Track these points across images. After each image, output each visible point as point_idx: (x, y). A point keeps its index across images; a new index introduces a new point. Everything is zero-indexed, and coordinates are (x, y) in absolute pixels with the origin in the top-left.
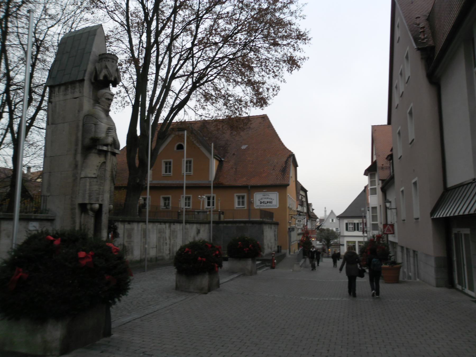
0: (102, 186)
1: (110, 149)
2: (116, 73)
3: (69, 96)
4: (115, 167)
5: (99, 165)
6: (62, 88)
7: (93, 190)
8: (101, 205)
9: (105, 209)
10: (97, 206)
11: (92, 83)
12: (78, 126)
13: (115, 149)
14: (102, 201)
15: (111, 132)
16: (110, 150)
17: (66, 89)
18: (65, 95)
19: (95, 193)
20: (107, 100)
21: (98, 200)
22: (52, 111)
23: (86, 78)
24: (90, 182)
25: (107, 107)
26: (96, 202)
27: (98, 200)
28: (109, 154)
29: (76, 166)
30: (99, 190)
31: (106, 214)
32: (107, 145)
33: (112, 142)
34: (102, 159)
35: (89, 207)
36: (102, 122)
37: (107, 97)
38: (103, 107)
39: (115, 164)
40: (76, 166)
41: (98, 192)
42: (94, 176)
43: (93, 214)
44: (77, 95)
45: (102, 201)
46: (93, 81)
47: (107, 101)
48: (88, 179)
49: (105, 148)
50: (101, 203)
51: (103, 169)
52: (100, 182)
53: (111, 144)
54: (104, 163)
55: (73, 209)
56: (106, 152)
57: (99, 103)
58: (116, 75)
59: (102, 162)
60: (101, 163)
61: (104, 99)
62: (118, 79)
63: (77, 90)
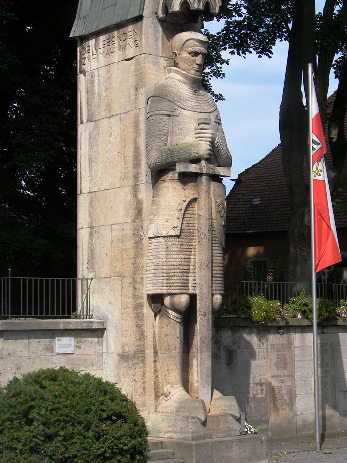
0: (193, 253)
3: (117, 56)
5: (184, 207)
6: (103, 38)
8: (193, 297)
9: (202, 306)
10: (184, 300)
11: (162, 21)
12: (136, 124)
13: (219, 166)
14: (194, 287)
17: (110, 41)
18: (109, 53)
19: (178, 271)
20: (193, 56)
21: (188, 286)
22: (88, 92)
23: (146, 12)
24: (168, 247)
25: (193, 72)
27: (185, 285)
28: (204, 179)
29: (139, 212)
32: (197, 160)
33: (208, 152)
34: (189, 192)
35: (167, 301)
37: (190, 49)
38: (185, 73)
40: (139, 212)
41: (185, 267)
42: (173, 233)
44: (130, 52)
45: (194, 287)
46: (161, 15)
47: (193, 58)
48: (161, 239)
49: (193, 168)
52: (188, 245)
53: (205, 157)
55: (138, 307)
57: (176, 65)
59: (188, 200)
60: (187, 203)
61: (185, 55)
63: (130, 41)
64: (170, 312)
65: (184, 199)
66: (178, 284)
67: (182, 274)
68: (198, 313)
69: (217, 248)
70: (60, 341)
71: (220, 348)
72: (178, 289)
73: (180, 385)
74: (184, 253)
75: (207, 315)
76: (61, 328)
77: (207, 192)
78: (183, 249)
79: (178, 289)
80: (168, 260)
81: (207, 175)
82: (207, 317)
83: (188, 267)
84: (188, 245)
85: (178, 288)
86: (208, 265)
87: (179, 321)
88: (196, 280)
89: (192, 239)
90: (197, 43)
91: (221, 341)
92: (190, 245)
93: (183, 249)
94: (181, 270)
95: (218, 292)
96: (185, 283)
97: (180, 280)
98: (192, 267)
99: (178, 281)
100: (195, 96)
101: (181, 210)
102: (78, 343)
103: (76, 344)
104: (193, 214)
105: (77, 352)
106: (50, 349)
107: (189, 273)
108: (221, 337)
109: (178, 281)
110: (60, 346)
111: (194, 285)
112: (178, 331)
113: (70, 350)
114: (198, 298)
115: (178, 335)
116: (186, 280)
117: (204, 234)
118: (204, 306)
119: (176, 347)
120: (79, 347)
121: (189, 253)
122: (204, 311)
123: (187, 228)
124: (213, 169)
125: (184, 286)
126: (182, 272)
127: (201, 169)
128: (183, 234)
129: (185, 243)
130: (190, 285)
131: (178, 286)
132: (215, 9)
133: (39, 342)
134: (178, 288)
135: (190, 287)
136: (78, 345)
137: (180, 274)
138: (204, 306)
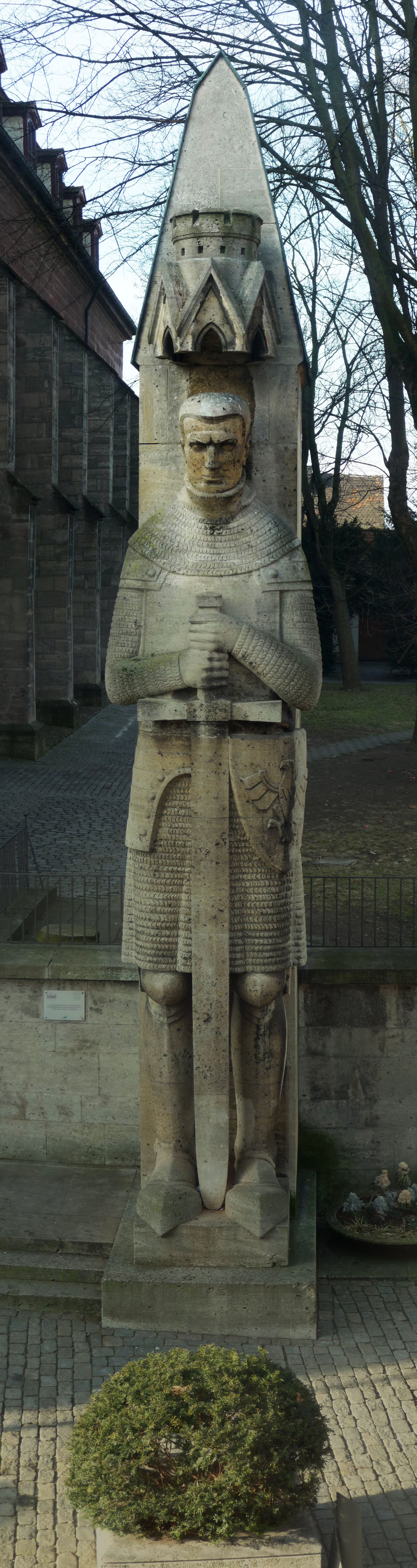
0: (184, 888)
8: (187, 978)
14: (185, 958)
20: (197, 450)
27: (166, 954)
31: (207, 1021)
45: (185, 958)
51: (182, 812)
52: (172, 871)
59: (168, 779)
62: (225, 329)
69: (254, 876)
70: (54, 997)
73: (172, 1145)
75: (213, 1021)
76: (46, 977)
77: (211, 761)
81: (208, 723)
82: (213, 1023)
84: (172, 871)
86: (215, 917)
88: (190, 945)
89: (183, 859)
90: (199, 424)
95: (258, 968)
98: (182, 917)
99: (148, 945)
100: (210, 538)
101: (153, 798)
102: (95, 1003)
103: (90, 1004)
104: (182, 808)
105: (94, 1018)
110: (54, 1007)
112: (165, 1041)
114: (194, 982)
115: (165, 1048)
116: (169, 943)
117: (204, 851)
118: (205, 1002)
119: (161, 1072)
120: (98, 1011)
122: (205, 1010)
125: (163, 956)
126: (158, 928)
127: (192, 712)
128: (160, 849)
129: (165, 869)
130: (180, 955)
132: (233, 343)
133: (8, 997)
136: (96, 1007)
137: (152, 932)
138: (205, 1002)
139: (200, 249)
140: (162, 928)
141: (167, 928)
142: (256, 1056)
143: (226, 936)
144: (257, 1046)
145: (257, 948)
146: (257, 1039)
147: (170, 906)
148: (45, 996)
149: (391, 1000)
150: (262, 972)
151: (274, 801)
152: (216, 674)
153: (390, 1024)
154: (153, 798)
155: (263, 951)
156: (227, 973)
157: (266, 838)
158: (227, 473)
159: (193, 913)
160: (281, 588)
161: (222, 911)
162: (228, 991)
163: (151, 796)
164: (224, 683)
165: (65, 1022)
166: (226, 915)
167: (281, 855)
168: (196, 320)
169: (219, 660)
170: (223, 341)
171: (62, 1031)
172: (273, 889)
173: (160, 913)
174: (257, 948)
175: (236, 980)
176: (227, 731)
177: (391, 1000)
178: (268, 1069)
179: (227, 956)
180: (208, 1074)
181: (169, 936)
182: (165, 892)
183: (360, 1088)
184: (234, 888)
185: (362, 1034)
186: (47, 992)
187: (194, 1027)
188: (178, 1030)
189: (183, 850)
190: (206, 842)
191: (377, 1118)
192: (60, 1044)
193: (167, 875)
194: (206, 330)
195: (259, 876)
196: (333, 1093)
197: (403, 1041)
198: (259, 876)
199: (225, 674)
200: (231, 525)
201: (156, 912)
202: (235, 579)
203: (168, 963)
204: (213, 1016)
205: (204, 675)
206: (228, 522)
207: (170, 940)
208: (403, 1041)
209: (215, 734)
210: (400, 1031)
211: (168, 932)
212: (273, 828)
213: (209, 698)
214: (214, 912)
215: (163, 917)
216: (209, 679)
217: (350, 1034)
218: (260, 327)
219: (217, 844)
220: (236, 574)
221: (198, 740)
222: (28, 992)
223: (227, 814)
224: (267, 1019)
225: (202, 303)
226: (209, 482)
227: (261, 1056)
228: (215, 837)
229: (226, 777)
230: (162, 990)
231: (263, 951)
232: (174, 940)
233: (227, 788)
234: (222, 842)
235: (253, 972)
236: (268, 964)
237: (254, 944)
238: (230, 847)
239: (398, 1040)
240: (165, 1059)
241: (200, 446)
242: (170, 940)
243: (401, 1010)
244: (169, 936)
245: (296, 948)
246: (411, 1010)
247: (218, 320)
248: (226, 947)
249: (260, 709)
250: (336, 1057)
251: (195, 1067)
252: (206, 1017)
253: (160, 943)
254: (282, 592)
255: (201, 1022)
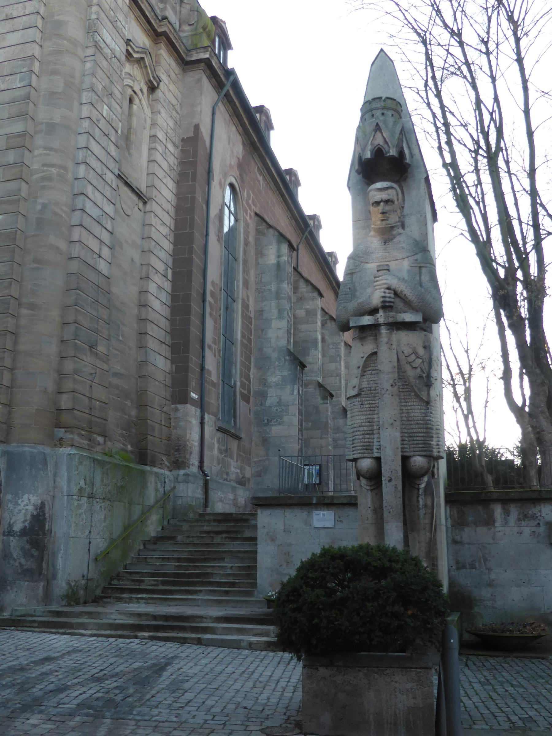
0: (376, 412)
1: (381, 317)
2: (379, 135)
4: (413, 357)
7: (355, 425)
8: (378, 460)
14: (378, 449)
15: (379, 277)
16: (381, 321)
19: (359, 433)
20: (375, 207)
21: (372, 450)
25: (379, 222)
26: (364, 453)
27: (368, 448)
30: (367, 424)
34: (369, 347)
36: (367, 263)
37: (372, 201)
39: (407, 351)
43: (367, 485)
45: (378, 449)
49: (367, 320)
50: (376, 455)
51: (374, 372)
52: (369, 404)
53: (380, 305)
54: (376, 353)
56: (375, 327)
58: (379, 140)
59: (366, 356)
60: (364, 359)
61: (372, 208)
62: (386, 146)
64: (361, 478)
65: (362, 356)
66: (359, 448)
67: (362, 436)
68: (383, 479)
69: (412, 404)
70: (318, 514)
71: (539, 524)
72: (359, 453)
74: (365, 413)
75: (393, 481)
76: (314, 502)
77: (387, 343)
78: (363, 410)
79: (359, 453)
80: (353, 422)
81: (385, 324)
82: (393, 483)
83: (371, 428)
84: (369, 404)
85: (359, 451)
86: (392, 424)
87: (368, 488)
91: (540, 516)
92: (372, 404)
93: (363, 410)
94: (361, 433)
96: (367, 446)
97: (361, 442)
98: (375, 428)
99: (359, 444)
100: (384, 246)
102: (340, 518)
103: (337, 518)
104: (373, 370)
106: (308, 523)
107: (373, 434)
108: (540, 511)
109: (359, 444)
111: (378, 447)
113: (330, 524)
114: (382, 461)
116: (369, 442)
117: (385, 390)
119: (368, 518)
120: (341, 521)
121: (371, 412)
123: (367, 386)
124: (393, 317)
125: (367, 449)
126: (363, 435)
128: (363, 393)
129: (366, 403)
130: (375, 447)
131: (359, 450)
132: (389, 152)
134: (359, 451)
135: (375, 450)
136: (340, 520)
137: (361, 437)
139: (373, 115)
140: (365, 434)
141: (368, 434)
142: (418, 506)
143: (398, 434)
144: (418, 501)
145: (415, 442)
146: (418, 497)
147: (369, 422)
148: (314, 514)
149: (498, 510)
150: (419, 456)
151: (421, 363)
152: (387, 299)
153: (497, 524)
154: (359, 367)
155: (419, 444)
156: (400, 454)
157: (417, 382)
158: (390, 216)
159: (381, 423)
160: (419, 265)
161: (395, 421)
162: (400, 464)
163: (358, 366)
164: (392, 304)
165: (325, 528)
166: (398, 423)
167: (426, 393)
168: (372, 144)
169: (389, 293)
170: (384, 151)
171: (323, 532)
172: (423, 411)
173: (364, 426)
174: (415, 442)
175: (405, 459)
176: (395, 328)
177: (498, 510)
178: (425, 514)
179: (400, 446)
180: (391, 510)
181: (369, 439)
182: (366, 415)
183: (482, 562)
184: (402, 410)
185: (482, 530)
186: (315, 512)
187: (383, 485)
188: (376, 494)
189: (374, 392)
190: (386, 385)
191: (493, 581)
192: (322, 541)
193: (367, 406)
194: (376, 148)
195: (415, 404)
196: (468, 566)
197: (505, 534)
198: (415, 404)
199: (392, 300)
200: (394, 240)
201: (362, 426)
202: (396, 262)
203: (369, 453)
204: (393, 478)
205: (382, 299)
206: (392, 239)
207: (370, 440)
208: (505, 534)
209: (388, 330)
210: (503, 528)
211: (368, 436)
212: (421, 377)
213: (385, 312)
214: (392, 421)
215: (365, 428)
216: (384, 302)
217: (475, 531)
218: (402, 148)
219: (392, 385)
220: (397, 260)
221: (380, 334)
222: (305, 513)
223: (396, 370)
224: (423, 486)
225: (374, 136)
226: (382, 220)
227: (421, 506)
228: (391, 382)
229: (395, 351)
230: (366, 469)
231: (419, 444)
232: (372, 440)
233: (395, 357)
234: (394, 384)
235: (414, 456)
236: (422, 451)
237: (414, 440)
238: (399, 388)
239: (501, 533)
240: (369, 509)
241: (377, 203)
242: (370, 440)
243: (503, 516)
244: (369, 439)
245: (437, 447)
246: (509, 516)
247: (381, 142)
248: (399, 439)
249: (411, 315)
250: (469, 544)
251: (384, 506)
252: (389, 479)
253: (365, 442)
254: (420, 267)
255: (387, 482)
